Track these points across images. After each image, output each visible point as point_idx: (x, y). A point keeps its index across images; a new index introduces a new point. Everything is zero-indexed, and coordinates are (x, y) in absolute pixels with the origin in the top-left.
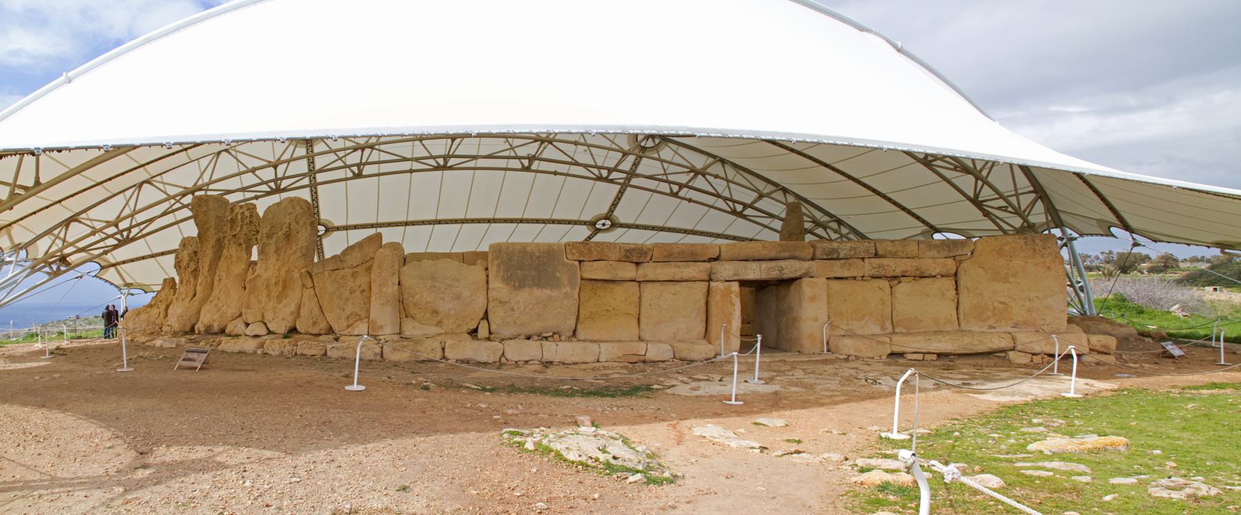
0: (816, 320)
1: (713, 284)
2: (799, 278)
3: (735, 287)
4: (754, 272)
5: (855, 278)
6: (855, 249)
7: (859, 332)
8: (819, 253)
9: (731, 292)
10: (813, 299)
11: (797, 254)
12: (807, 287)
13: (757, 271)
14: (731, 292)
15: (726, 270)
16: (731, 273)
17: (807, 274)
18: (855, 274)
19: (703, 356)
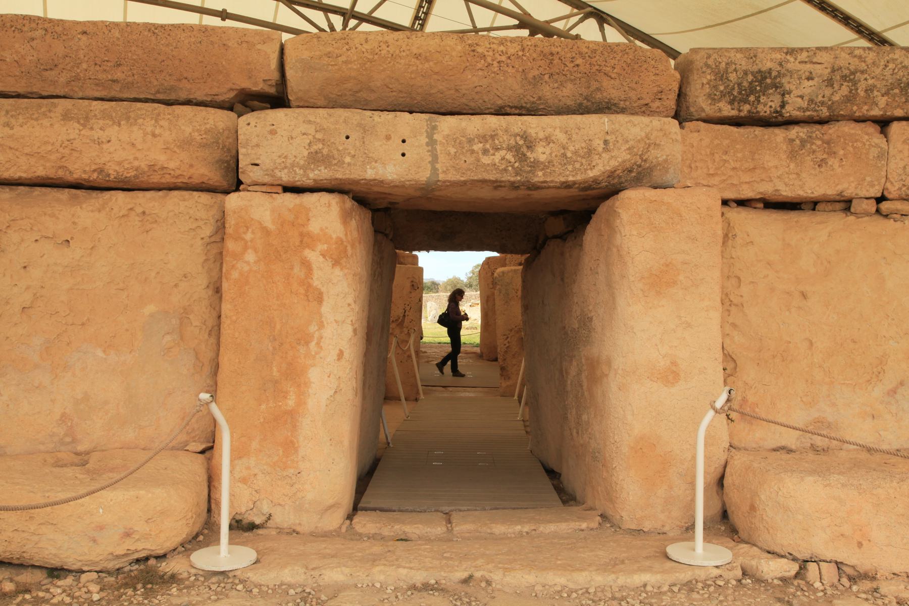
0: (671, 375)
1: (233, 200)
2: (612, 192)
3: (327, 216)
4: (404, 154)
5: (846, 204)
6: (850, 77)
7: (862, 432)
8: (700, 99)
9: (307, 240)
10: (661, 281)
11: (612, 91)
12: (637, 233)
13: (418, 149)
14: (307, 240)
15: (274, 141)
16: (299, 150)
17: (640, 175)
18: (849, 188)
19: (109, 548)
